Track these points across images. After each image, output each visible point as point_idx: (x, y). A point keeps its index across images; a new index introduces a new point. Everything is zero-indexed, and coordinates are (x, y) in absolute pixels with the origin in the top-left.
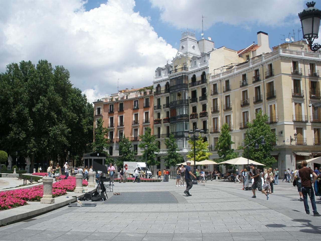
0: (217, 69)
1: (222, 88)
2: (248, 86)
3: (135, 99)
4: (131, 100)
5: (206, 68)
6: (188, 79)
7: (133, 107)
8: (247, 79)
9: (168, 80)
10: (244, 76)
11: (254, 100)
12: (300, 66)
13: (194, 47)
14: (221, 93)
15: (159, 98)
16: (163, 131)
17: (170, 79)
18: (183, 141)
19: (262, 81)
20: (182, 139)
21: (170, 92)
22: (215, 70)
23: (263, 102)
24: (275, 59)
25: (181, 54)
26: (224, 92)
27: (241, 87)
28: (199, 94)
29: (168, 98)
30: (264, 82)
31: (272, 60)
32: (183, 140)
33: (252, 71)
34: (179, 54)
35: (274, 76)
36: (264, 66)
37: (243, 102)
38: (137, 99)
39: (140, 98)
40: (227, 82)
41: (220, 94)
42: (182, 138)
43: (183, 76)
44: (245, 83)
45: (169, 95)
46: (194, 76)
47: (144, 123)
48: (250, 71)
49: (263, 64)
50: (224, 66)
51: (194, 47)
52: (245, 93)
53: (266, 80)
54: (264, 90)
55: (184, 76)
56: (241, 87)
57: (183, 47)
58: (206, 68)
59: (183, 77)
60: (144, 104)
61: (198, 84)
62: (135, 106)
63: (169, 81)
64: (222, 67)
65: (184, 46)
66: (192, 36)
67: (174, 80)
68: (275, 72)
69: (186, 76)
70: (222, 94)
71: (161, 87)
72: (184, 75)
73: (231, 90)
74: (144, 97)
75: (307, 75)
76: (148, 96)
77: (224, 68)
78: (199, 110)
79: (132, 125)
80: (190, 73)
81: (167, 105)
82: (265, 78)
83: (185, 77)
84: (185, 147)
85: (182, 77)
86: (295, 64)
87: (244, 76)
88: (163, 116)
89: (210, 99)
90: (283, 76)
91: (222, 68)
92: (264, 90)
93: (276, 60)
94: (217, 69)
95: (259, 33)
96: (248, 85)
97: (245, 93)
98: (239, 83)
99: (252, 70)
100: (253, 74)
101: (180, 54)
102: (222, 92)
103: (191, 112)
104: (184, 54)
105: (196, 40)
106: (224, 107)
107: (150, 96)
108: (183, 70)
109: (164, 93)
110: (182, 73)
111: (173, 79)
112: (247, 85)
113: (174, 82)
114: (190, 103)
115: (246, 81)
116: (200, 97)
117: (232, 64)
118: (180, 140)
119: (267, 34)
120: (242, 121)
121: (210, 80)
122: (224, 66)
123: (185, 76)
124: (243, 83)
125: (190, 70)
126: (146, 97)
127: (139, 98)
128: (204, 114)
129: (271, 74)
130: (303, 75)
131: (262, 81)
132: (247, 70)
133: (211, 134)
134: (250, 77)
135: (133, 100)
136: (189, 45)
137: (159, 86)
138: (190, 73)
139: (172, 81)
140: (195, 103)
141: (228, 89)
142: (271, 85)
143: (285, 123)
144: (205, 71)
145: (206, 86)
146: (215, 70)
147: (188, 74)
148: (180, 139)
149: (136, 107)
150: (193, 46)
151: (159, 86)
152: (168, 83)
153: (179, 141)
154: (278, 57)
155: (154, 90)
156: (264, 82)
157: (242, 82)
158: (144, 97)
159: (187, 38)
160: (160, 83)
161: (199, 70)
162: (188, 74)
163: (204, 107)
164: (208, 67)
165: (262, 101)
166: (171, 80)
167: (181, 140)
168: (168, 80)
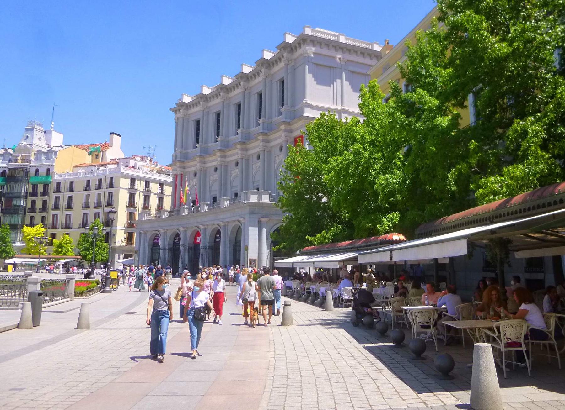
1: (66, 188)
10: (88, 182)
12: (137, 182)
13: (40, 139)
28: (40, 189)
34: (22, 143)
41: (63, 193)
42: (15, 231)
44: (88, 188)
51: (40, 139)
57: (27, 137)
65: (29, 136)
66: (39, 125)
68: (114, 185)
72: (25, 167)
75: (142, 190)
78: (39, 205)
84: (18, 239)
86: (133, 180)
89: (53, 195)
90: (121, 190)
95: (112, 134)
98: (83, 187)
101: (23, 144)
102: (66, 191)
103: (29, 206)
104: (29, 144)
105: (43, 131)
106: (65, 206)
111: (12, 168)
112: (89, 190)
114: (30, 196)
116: (41, 192)
119: (120, 136)
120: (81, 222)
124: (86, 188)
125: (32, 164)
128: (44, 208)
129: (111, 186)
130: (139, 189)
134: (93, 184)
136: (35, 135)
140: (35, 197)
141: (71, 189)
142: (110, 194)
143: (118, 228)
144: (50, 167)
150: (39, 137)
152: (5, 171)
157: (85, 186)
163: (45, 202)
166: (9, 169)
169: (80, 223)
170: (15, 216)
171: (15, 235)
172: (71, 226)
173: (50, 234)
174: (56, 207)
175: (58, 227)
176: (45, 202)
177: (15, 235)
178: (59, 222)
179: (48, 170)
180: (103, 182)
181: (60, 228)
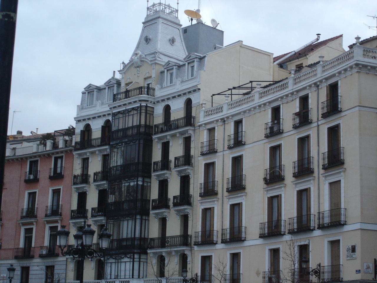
0: (218, 94)
2: (284, 135)
3: (31, 157)
4: (22, 159)
5: (194, 91)
6: (153, 114)
7: (26, 176)
8: (281, 118)
9: (109, 114)
10: (276, 111)
11: (295, 168)
15: (87, 157)
17: (113, 113)
18: (133, 262)
19: (315, 124)
20: (130, 258)
21: (111, 143)
22: (214, 95)
23: (314, 175)
24: (345, 70)
25: (140, 56)
26: (230, 148)
29: (106, 159)
30: (318, 126)
31: (340, 73)
32: (132, 260)
33: (293, 100)
35: (341, 111)
36: (320, 87)
37: (270, 174)
38: (35, 157)
39: (44, 155)
40: (238, 123)
41: (221, 153)
43: (141, 106)
44: (275, 129)
45: (108, 150)
46: (167, 109)
47: (49, 216)
48: (290, 99)
49: (318, 83)
50: (234, 88)
51: (172, 41)
52: (275, 150)
53: (323, 121)
54: (317, 145)
55: (144, 108)
56: (267, 137)
58: (194, 91)
59: (141, 110)
60: (51, 169)
61: (177, 127)
62: (30, 173)
63: (110, 118)
64: (229, 89)
67: (121, 116)
69: (148, 109)
70: (225, 153)
72: (144, 104)
73: (244, 144)
74: (53, 154)
76: (62, 152)
77: (234, 91)
80: (158, 102)
82: (320, 116)
83: (146, 110)
85: (139, 109)
87: (276, 111)
89: (200, 163)
91: (229, 92)
92: (319, 146)
93: (348, 73)
94: (218, 94)
96: (282, 133)
97: (275, 150)
98: (264, 127)
99: (294, 97)
100: (296, 106)
106: (228, 183)
107: (66, 151)
108: (141, 94)
109: (98, 146)
110: (140, 101)
111: (119, 112)
112: (280, 132)
113: (121, 121)
115: (279, 123)
117: (251, 82)
118: (126, 259)
121: (201, 118)
122: (234, 88)
123: (146, 106)
124: (271, 128)
126: (57, 153)
127: (40, 156)
131: (315, 124)
132: (282, 98)
133: (196, 248)
135: (26, 158)
137: (88, 127)
138: (158, 102)
139: (116, 117)
145: (191, 132)
146: (214, 95)
147: (154, 103)
148: (126, 256)
149: (32, 177)
150: (170, 37)
151: (87, 129)
152: (108, 122)
153: (122, 260)
154: (351, 67)
155: (77, 138)
157: (270, 125)
158: (53, 154)
159: (159, 17)
160: (90, 122)
161: (179, 96)
162: (154, 103)
163: (185, 181)
164: (199, 89)
165: (312, 172)
166: (114, 115)
167: (129, 260)
168: (109, 114)
169: (263, 224)
170: (128, 220)
171: (128, 264)
172: (243, 235)
175: (215, 239)
176: (185, 181)
177: (128, 264)
178: (217, 226)
179: (189, 103)
180: (312, 103)
181: (220, 241)
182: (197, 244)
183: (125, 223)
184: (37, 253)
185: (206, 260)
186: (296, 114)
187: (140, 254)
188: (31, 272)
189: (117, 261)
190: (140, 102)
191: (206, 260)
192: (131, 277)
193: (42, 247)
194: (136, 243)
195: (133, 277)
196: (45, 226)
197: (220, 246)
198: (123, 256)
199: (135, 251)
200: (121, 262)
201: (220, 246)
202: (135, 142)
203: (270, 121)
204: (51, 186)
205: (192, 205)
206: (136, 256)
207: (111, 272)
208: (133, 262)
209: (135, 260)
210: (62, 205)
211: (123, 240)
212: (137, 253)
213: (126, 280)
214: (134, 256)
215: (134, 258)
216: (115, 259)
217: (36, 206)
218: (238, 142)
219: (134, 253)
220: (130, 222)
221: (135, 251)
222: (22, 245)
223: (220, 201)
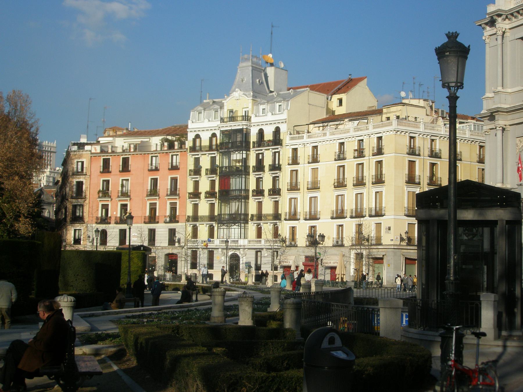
1: (307, 157)
14: (304, 164)
16: (204, 210)
20: (238, 226)
27: (335, 160)
30: (369, 159)
32: (239, 227)
44: (341, 156)
47: (169, 196)
71: (202, 139)
79: (146, 196)
81: (213, 171)
88: (204, 186)
98: (334, 154)
112: (344, 159)
115: (343, 153)
118: (235, 227)
124: (339, 156)
156: (369, 159)
167: (237, 227)
173: (290, 227)
174: (294, 187)
177: (237, 230)
181: (302, 218)
182: (286, 220)
183: (234, 204)
184: (162, 219)
185: (293, 230)
186: (355, 150)
187: (244, 223)
188: (156, 233)
189: (228, 228)
190: (243, 126)
191: (293, 230)
192: (239, 238)
193: (165, 216)
194: (242, 217)
195: (240, 238)
196: (167, 202)
197: (302, 221)
198: (233, 225)
199: (242, 222)
200: (231, 228)
201: (302, 221)
202: (240, 152)
203: (338, 151)
204: (170, 175)
205: (281, 195)
206: (243, 225)
207: (229, 235)
208: (241, 228)
209: (242, 227)
210: (179, 188)
211: (232, 214)
212: (243, 223)
213: (235, 239)
214: (241, 225)
215: (241, 226)
216: (227, 226)
217: (158, 188)
218: (315, 160)
219: (241, 223)
220: (237, 203)
221: (242, 222)
222: (148, 214)
223: (302, 194)
